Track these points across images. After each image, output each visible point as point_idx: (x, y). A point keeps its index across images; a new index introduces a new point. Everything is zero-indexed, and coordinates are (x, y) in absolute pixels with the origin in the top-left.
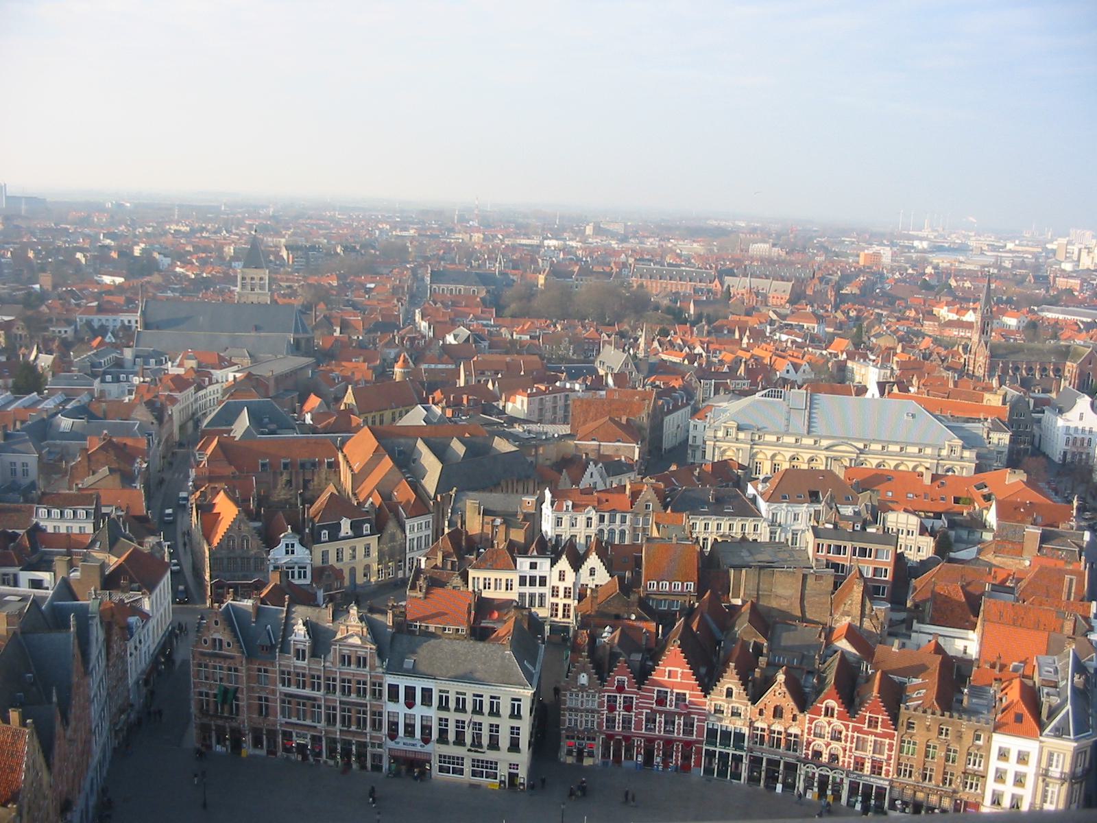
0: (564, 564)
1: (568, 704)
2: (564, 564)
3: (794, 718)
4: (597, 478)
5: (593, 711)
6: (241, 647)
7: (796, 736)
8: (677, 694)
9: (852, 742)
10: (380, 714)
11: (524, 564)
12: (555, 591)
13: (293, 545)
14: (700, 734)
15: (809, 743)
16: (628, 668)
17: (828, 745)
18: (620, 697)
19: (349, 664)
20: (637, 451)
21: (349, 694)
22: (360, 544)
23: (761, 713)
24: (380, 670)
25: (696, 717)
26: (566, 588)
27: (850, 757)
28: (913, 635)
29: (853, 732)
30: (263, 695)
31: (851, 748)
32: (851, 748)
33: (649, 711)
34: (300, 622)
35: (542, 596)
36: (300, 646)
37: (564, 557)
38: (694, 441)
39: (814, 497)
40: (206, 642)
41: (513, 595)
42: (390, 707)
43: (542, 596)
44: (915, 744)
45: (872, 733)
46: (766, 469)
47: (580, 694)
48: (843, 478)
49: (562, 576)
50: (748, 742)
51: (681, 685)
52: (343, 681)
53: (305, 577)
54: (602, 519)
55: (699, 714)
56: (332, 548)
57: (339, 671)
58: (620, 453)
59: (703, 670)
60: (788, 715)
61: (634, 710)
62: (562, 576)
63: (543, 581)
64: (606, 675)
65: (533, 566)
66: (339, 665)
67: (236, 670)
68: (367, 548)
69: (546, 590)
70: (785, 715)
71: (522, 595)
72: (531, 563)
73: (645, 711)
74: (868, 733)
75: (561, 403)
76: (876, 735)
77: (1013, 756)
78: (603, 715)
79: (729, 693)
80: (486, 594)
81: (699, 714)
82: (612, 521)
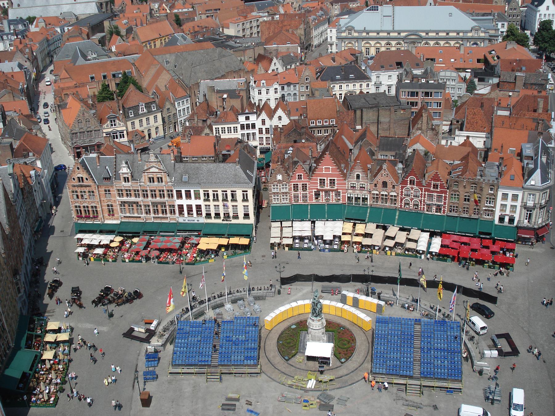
0: (264, 116)
1: (273, 191)
2: (264, 116)
3: (394, 187)
5: (286, 193)
6: (93, 180)
7: (395, 196)
8: (330, 180)
10: (174, 206)
11: (242, 119)
12: (261, 131)
15: (402, 200)
16: (303, 168)
17: (412, 199)
19: (154, 182)
20: (299, 48)
21: (156, 197)
23: (376, 185)
24: (170, 184)
25: (341, 191)
26: (266, 129)
27: (424, 205)
30: (110, 203)
31: (424, 200)
32: (424, 200)
34: (124, 162)
35: (254, 134)
36: (126, 176)
39: (399, 64)
40: (74, 179)
41: (238, 135)
42: (178, 202)
43: (254, 134)
45: (435, 192)
46: (373, 52)
47: (279, 185)
48: (414, 54)
49: (263, 122)
50: (370, 201)
52: (151, 191)
53: (124, 137)
54: (283, 88)
57: (149, 186)
58: (290, 50)
59: (343, 165)
60: (389, 186)
62: (263, 122)
63: (254, 126)
66: (149, 184)
68: (155, 117)
69: (256, 131)
70: (388, 186)
71: (243, 135)
73: (314, 190)
74: (433, 192)
76: (437, 192)
77: (510, 197)
78: (292, 194)
79: (358, 177)
80: (223, 136)
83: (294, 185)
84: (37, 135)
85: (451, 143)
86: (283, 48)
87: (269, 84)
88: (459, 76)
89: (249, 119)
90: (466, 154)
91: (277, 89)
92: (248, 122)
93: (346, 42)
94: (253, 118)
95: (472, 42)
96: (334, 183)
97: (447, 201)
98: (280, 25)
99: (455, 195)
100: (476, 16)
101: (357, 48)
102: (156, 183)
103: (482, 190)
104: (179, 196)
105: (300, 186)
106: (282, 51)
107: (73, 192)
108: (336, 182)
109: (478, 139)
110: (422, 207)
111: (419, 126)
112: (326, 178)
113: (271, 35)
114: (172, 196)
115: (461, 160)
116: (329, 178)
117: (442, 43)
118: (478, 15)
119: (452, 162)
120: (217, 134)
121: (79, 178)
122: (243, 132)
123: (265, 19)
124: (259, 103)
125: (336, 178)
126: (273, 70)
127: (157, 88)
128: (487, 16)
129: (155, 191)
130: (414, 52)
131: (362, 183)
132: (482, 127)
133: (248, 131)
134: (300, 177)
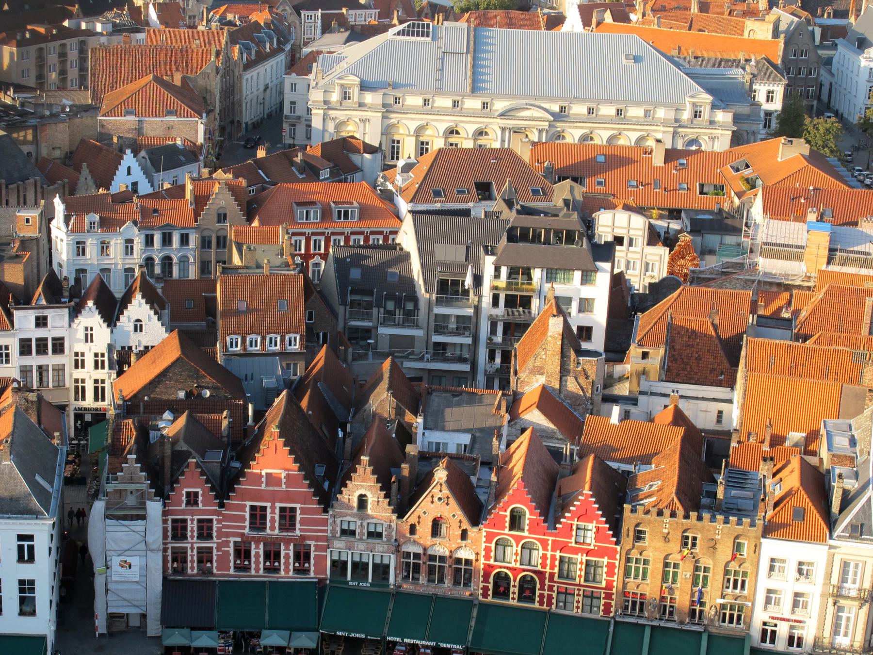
3: (464, 535)
4: (138, 175)
7: (468, 562)
8: (282, 509)
9: (552, 567)
14: (320, 569)
18: (192, 520)
20: (201, 129)
23: (413, 529)
25: (313, 543)
28: (642, 399)
29: (553, 550)
33: (239, 539)
37: (90, 303)
38: (294, 110)
43: (60, 370)
44: (646, 562)
49: (89, 338)
50: (396, 577)
51: (288, 497)
55: (317, 539)
58: (173, 133)
59: (320, 471)
61: (215, 539)
64: (167, 487)
65: (41, 322)
72: (37, 318)
73: (232, 539)
75: (73, 55)
81: (317, 539)
82: (167, 240)
89: (45, 324)
92: (41, 333)
96: (293, 518)
97: (615, 578)
103: (714, 548)
105: (192, 526)
109: (703, 405)
110: (546, 593)
111: (538, 363)
112: (268, 505)
122: (28, 361)
124: (78, 280)
132: (713, 370)
133: (42, 360)
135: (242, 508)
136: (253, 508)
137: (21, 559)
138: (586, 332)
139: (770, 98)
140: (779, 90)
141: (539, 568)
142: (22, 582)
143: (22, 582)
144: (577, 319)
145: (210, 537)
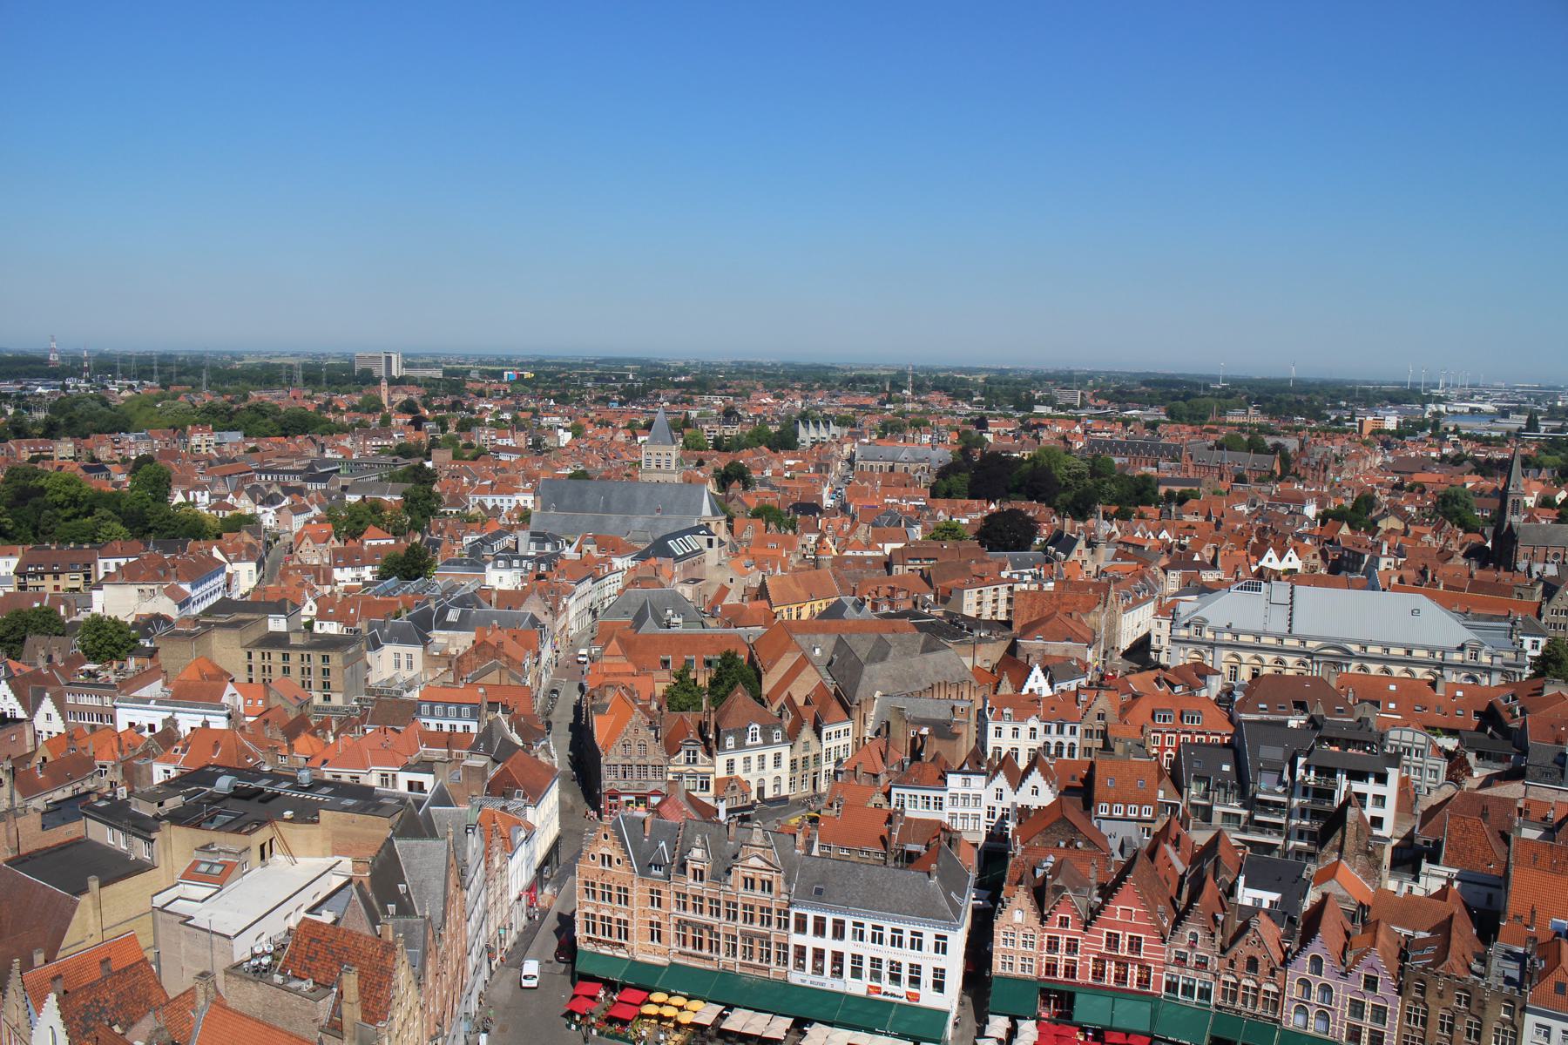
0: (1001, 781)
2: (1001, 781)
3: (1272, 972)
8: (1131, 937)
9: (1344, 1006)
10: (786, 947)
13: (695, 753)
19: (753, 887)
21: (752, 921)
22: (770, 754)
23: (1232, 964)
25: (1153, 966)
27: (1341, 1024)
28: (1422, 879)
30: (655, 919)
31: (1343, 1013)
32: (1343, 1013)
35: (977, 817)
36: (698, 866)
40: (593, 857)
42: (795, 939)
46: (1245, 675)
47: (1016, 933)
51: (1136, 928)
52: (745, 907)
54: (1047, 730)
55: (1155, 963)
56: (739, 758)
57: (743, 896)
58: (1070, 655)
60: (1263, 968)
63: (978, 798)
65: (966, 783)
66: (742, 889)
67: (626, 890)
68: (778, 757)
69: (983, 813)
70: (1260, 969)
71: (953, 816)
73: (1092, 956)
78: (1041, 958)
81: (1155, 963)
82: (1060, 731)
83: (1049, 937)
84: (536, 757)
85: (1410, 889)
86: (1057, 648)
87: (1021, 717)
88: (1432, 742)
90: (1445, 917)
91: (1033, 729)
93: (1189, 650)
94: (978, 781)
95: (1463, 674)
96: (1139, 945)
98: (1055, 602)
99: (1417, 1010)
100: (1474, 620)
101: (1210, 665)
102: (758, 891)
104: (801, 927)
105: (1063, 943)
106: (1054, 654)
107: (587, 883)
108: (1143, 945)
113: (1034, 619)
114: (787, 926)
115: (1432, 930)
116: (1128, 934)
117: (1397, 670)
118: (1477, 617)
119: (1410, 933)
120: (899, 808)
121: (603, 856)
123: (1025, 586)
124: (994, 755)
125: (1143, 936)
126: (1031, 691)
127: (790, 699)
128: (1499, 621)
129: (752, 908)
130: (1333, 684)
131: (1201, 954)
134: (1064, 922)
135: (1101, 933)
136: (1108, 934)
137: (937, 951)
138: (1377, 822)
139: (1535, 646)
140: (1542, 642)
141: (1333, 1006)
142: (935, 969)
143: (935, 969)
144: (1370, 811)
145: (1076, 951)
